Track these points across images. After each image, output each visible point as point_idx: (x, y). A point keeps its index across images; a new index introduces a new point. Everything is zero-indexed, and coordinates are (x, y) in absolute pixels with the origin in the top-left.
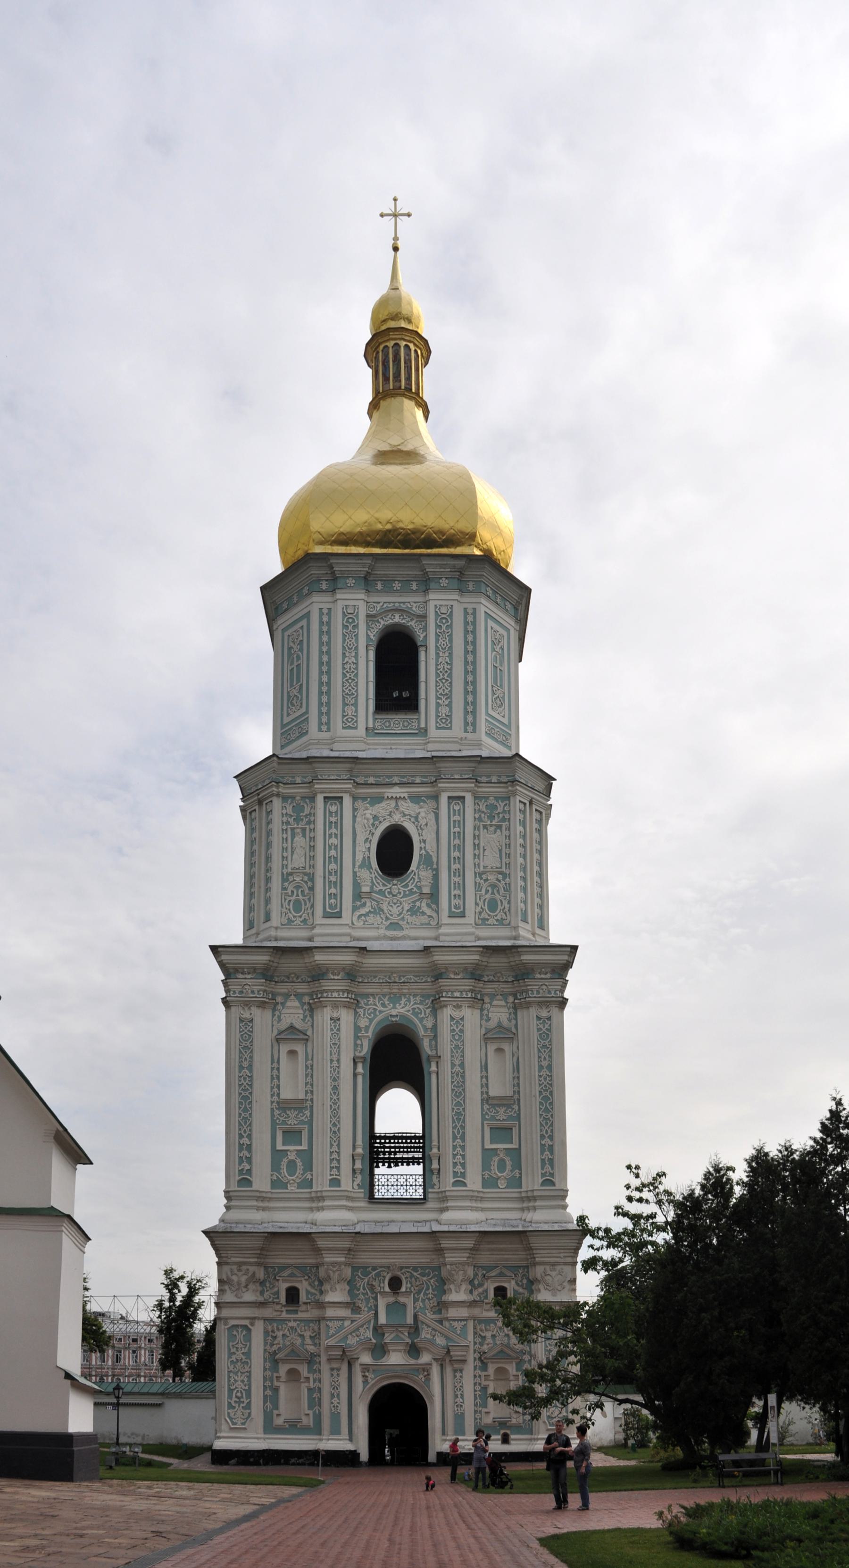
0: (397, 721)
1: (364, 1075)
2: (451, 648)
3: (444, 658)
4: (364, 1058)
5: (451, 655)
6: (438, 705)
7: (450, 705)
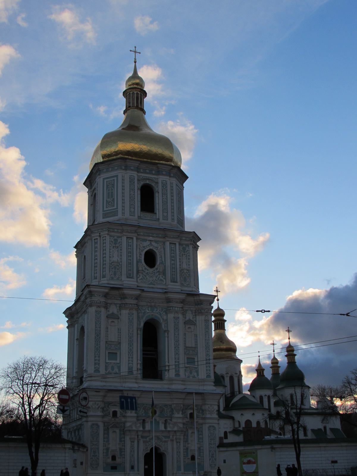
0: (148, 215)
1: (140, 334)
2: (167, 194)
4: (141, 328)
5: (167, 197)
6: (163, 212)
7: (167, 213)
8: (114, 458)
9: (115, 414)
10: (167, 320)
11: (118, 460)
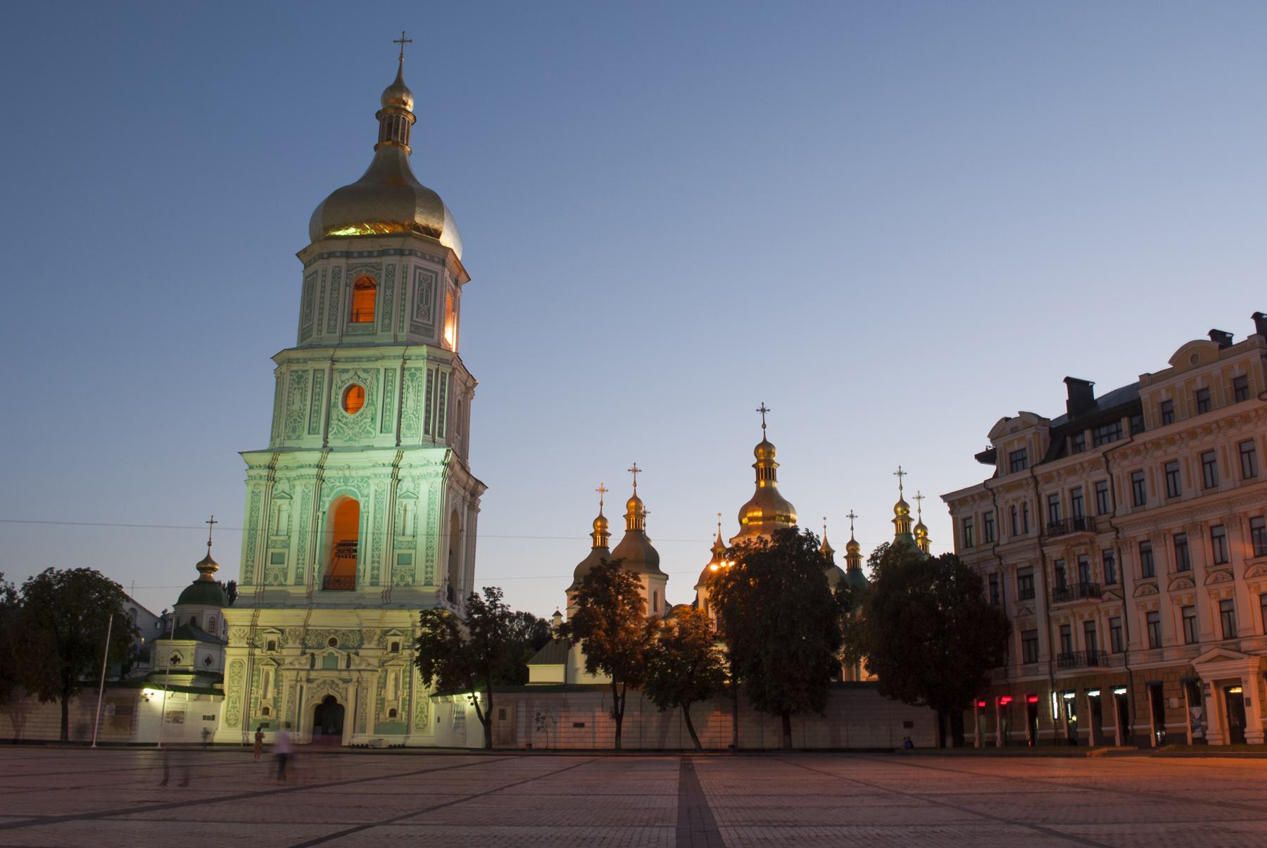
3: (389, 293)
8: (266, 711)
9: (271, 646)
10: (368, 496)
11: (273, 713)
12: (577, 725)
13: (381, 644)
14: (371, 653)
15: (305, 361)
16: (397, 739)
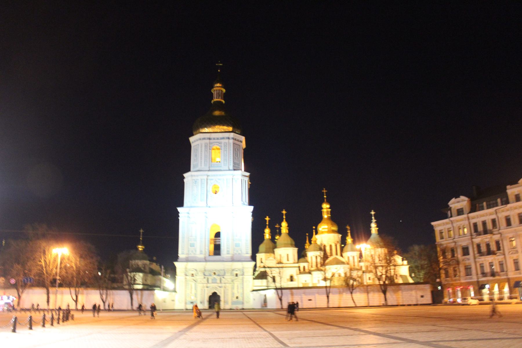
9: (193, 275)
12: (310, 300)
13: (232, 274)
14: (228, 277)
15: (197, 176)
16: (240, 307)
